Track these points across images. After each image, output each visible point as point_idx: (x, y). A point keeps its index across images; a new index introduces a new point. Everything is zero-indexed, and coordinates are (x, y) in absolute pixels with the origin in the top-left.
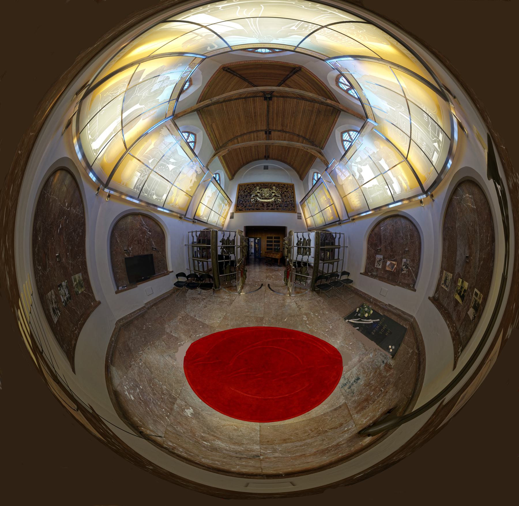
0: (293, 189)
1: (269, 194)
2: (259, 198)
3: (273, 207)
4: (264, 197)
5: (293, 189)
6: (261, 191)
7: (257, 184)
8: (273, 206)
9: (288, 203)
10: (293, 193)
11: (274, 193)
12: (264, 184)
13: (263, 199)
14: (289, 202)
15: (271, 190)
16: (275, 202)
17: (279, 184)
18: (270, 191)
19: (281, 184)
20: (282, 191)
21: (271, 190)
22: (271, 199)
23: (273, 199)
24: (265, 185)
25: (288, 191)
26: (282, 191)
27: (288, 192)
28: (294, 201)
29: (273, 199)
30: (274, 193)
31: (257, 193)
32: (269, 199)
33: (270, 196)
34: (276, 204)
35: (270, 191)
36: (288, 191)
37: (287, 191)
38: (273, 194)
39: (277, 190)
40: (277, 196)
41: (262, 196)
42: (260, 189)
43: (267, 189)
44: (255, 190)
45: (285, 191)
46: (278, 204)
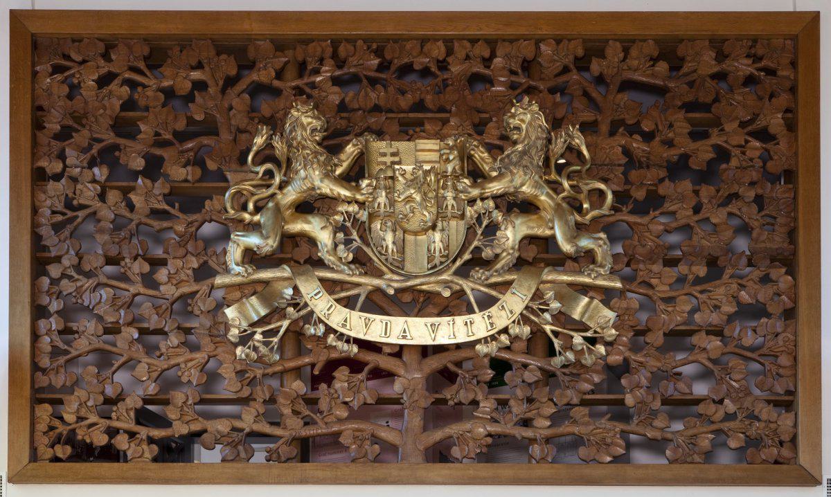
0: (791, 126)
1: (457, 229)
2: (330, 286)
3: (507, 427)
4: (398, 267)
5: (791, 126)
6: (353, 177)
7: (280, 45)
8: (518, 409)
9: (715, 343)
10: (790, 175)
11: (528, 207)
12: (378, 46)
13: (376, 304)
14: (717, 332)
15: (481, 155)
16: (540, 343)
17: (595, 49)
18: (477, 175)
19: (627, 45)
20: (632, 161)
21: (481, 155)
22: (486, 303)
23: (515, 302)
24: (407, 69)
25: (723, 155)
26: (632, 161)
27: (707, 175)
28: (790, 314)
29: (515, 302)
30: (528, 207)
31: (305, 207)
32: (455, 305)
33: (478, 261)
34: (549, 376)
35: (477, 175)
36: (723, 155)
37: (703, 153)
38: (512, 233)
39: (571, 150)
40: (559, 261)
41: (360, 261)
42: (331, 144)
43: (426, 152)
44: (267, 155)
45: (677, 168)
46: (576, 369)
